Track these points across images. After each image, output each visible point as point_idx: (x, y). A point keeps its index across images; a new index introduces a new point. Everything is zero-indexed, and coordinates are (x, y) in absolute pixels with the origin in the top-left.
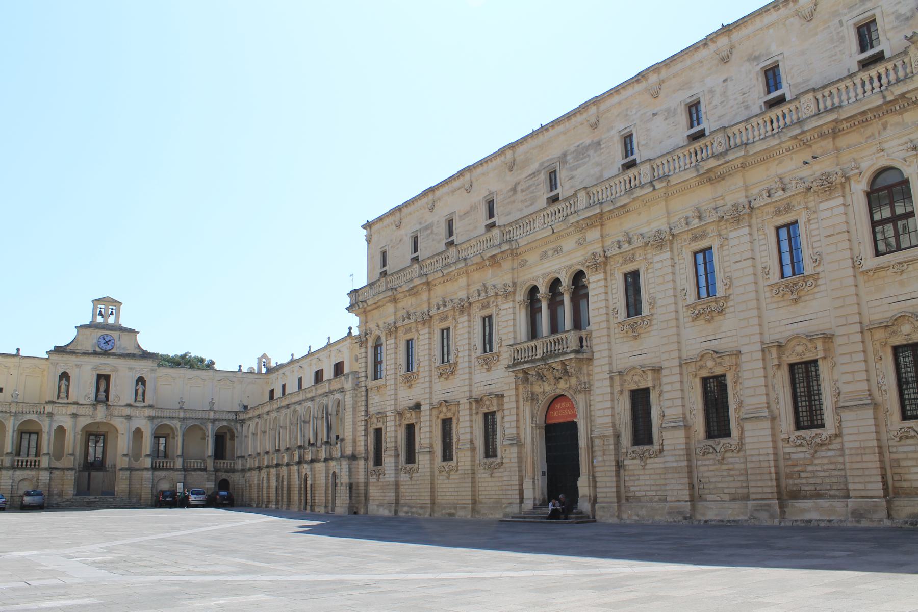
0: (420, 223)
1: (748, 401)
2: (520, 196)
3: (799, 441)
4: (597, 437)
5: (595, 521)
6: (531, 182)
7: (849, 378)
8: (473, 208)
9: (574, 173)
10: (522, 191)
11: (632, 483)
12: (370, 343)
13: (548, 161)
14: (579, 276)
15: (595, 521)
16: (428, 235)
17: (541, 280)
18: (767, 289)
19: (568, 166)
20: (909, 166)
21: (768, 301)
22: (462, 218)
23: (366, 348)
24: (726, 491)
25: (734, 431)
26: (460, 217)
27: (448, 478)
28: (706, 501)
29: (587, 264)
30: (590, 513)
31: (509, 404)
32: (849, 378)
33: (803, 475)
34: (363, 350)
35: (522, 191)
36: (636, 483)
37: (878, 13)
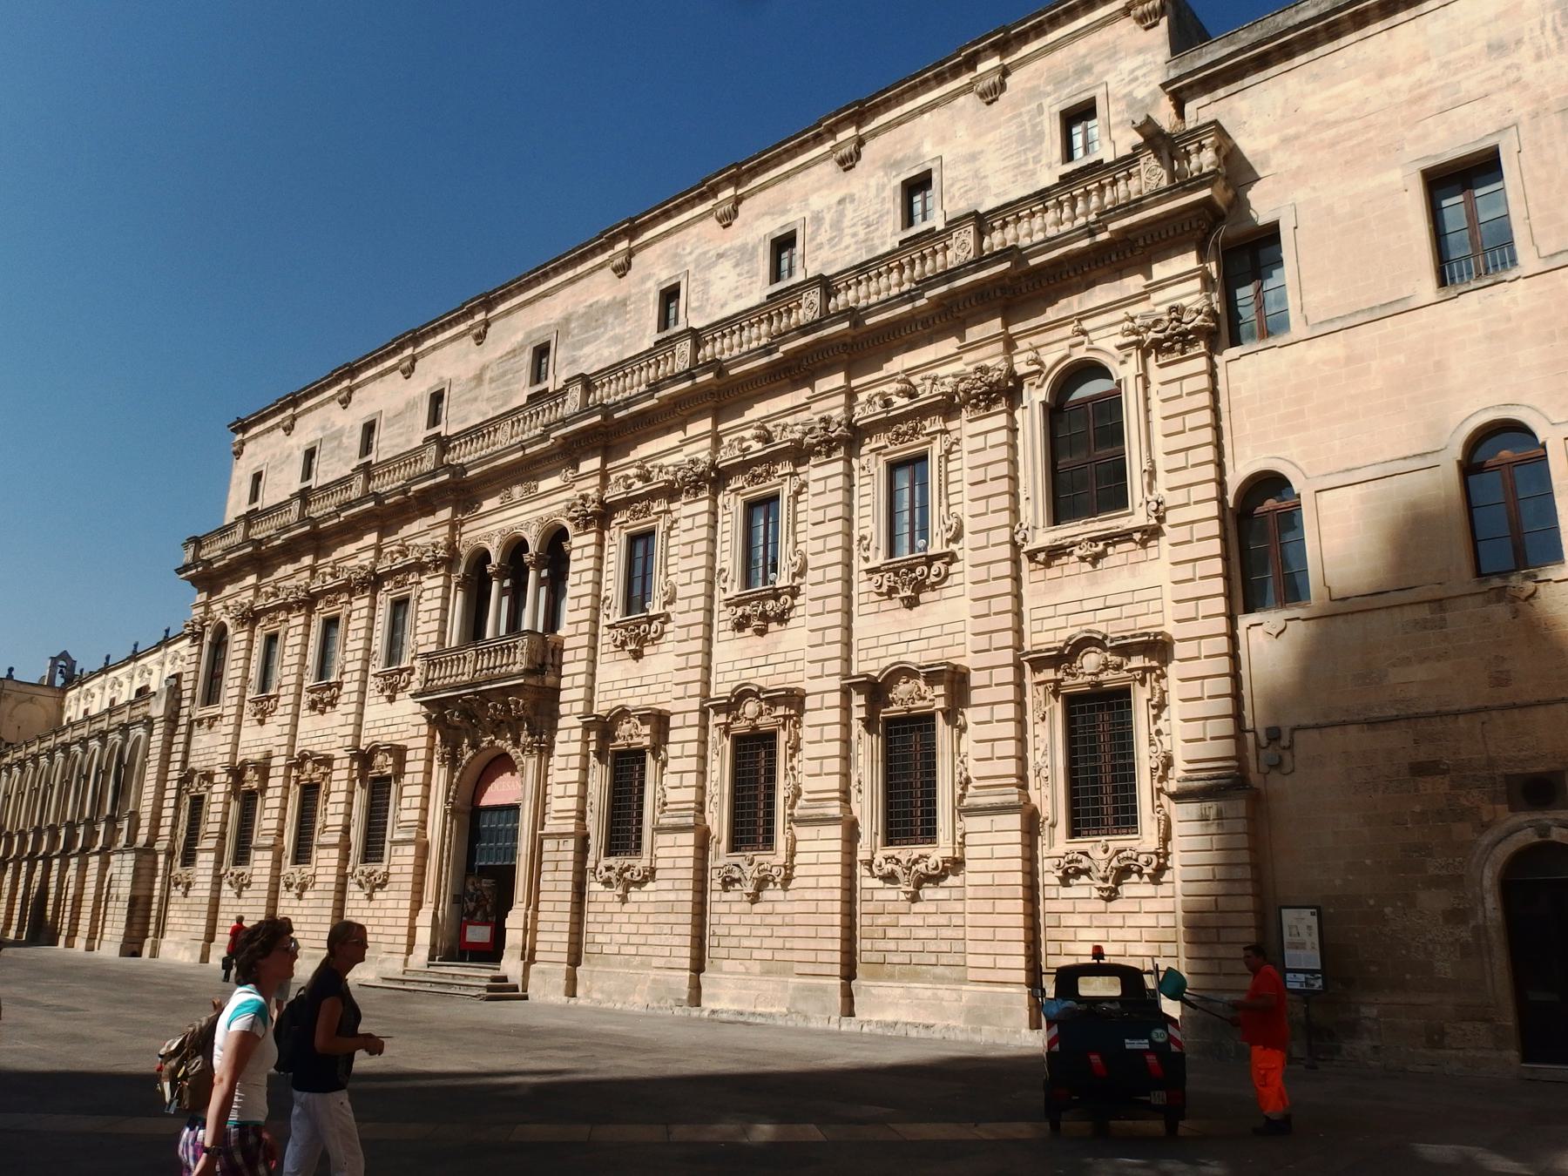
0: (323, 428)
1: (807, 784)
2: (486, 390)
3: (888, 867)
4: (551, 836)
5: (526, 998)
6: (507, 366)
7: (984, 750)
9: (578, 353)
10: (492, 380)
11: (598, 928)
12: (208, 637)
13: (539, 329)
14: (556, 539)
15: (526, 998)
16: (332, 451)
17: (496, 540)
18: (864, 576)
19: (569, 340)
20: (1123, 362)
21: (863, 598)
22: (391, 422)
23: (201, 645)
24: (756, 954)
25: (781, 842)
26: (387, 420)
27: (300, 897)
28: (720, 971)
29: (571, 514)
30: (519, 982)
31: (414, 765)
32: (984, 750)
33: (891, 933)
34: (195, 650)
35: (492, 380)
36: (607, 928)
37: (1099, 94)
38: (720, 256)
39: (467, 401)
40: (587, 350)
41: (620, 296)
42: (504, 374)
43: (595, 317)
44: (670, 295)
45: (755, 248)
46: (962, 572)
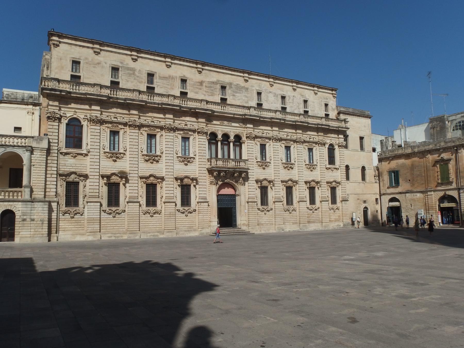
8: (171, 78)
10: (206, 87)
12: (65, 121)
13: (222, 81)
38: (270, 92)
39: (197, 88)
40: (237, 94)
41: (246, 87)
42: (211, 87)
43: (239, 88)
44: (259, 94)
45: (278, 95)
46: (318, 168)
